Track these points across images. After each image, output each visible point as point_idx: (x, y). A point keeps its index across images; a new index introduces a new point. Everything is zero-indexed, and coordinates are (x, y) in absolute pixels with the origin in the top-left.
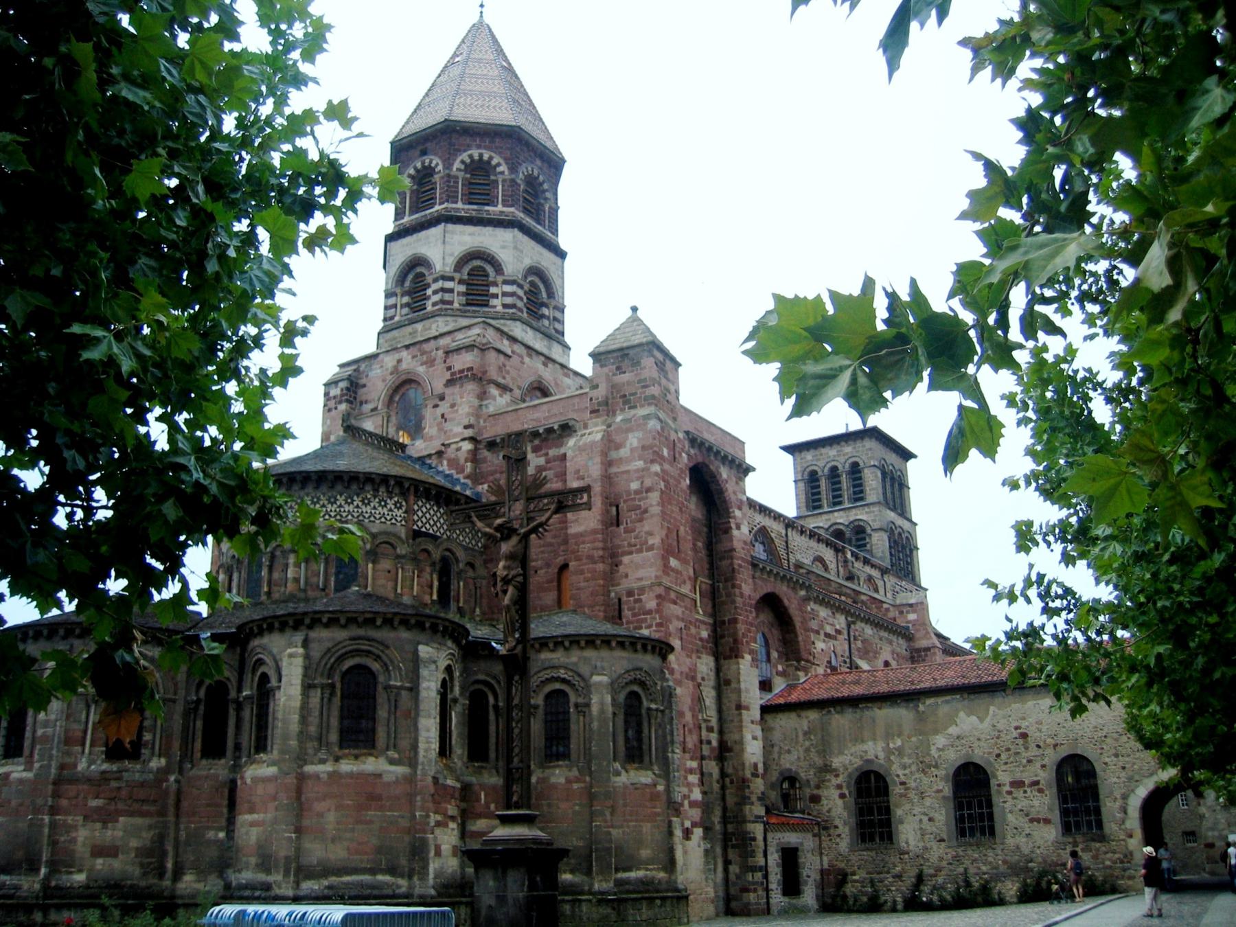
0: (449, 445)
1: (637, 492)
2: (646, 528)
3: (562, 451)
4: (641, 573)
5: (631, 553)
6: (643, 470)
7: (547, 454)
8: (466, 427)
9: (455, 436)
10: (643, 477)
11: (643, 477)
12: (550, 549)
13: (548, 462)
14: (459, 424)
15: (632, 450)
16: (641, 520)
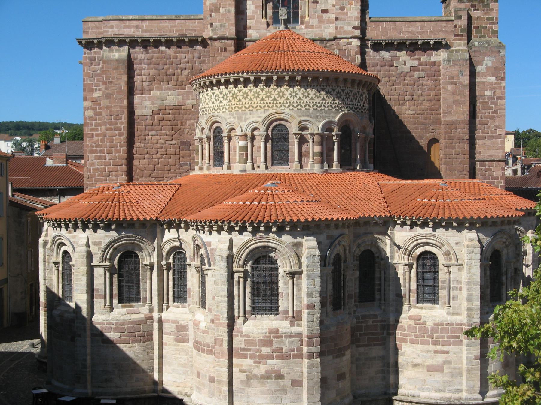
0: (341, 38)
1: (490, 98)
2: (497, 124)
3: (433, 59)
4: (491, 152)
5: (485, 138)
6: (495, 84)
7: (420, 59)
8: (355, 28)
9: (345, 32)
10: (495, 88)
11: (495, 88)
12: (422, 126)
13: (420, 64)
14: (349, 24)
15: (487, 68)
16: (493, 117)
